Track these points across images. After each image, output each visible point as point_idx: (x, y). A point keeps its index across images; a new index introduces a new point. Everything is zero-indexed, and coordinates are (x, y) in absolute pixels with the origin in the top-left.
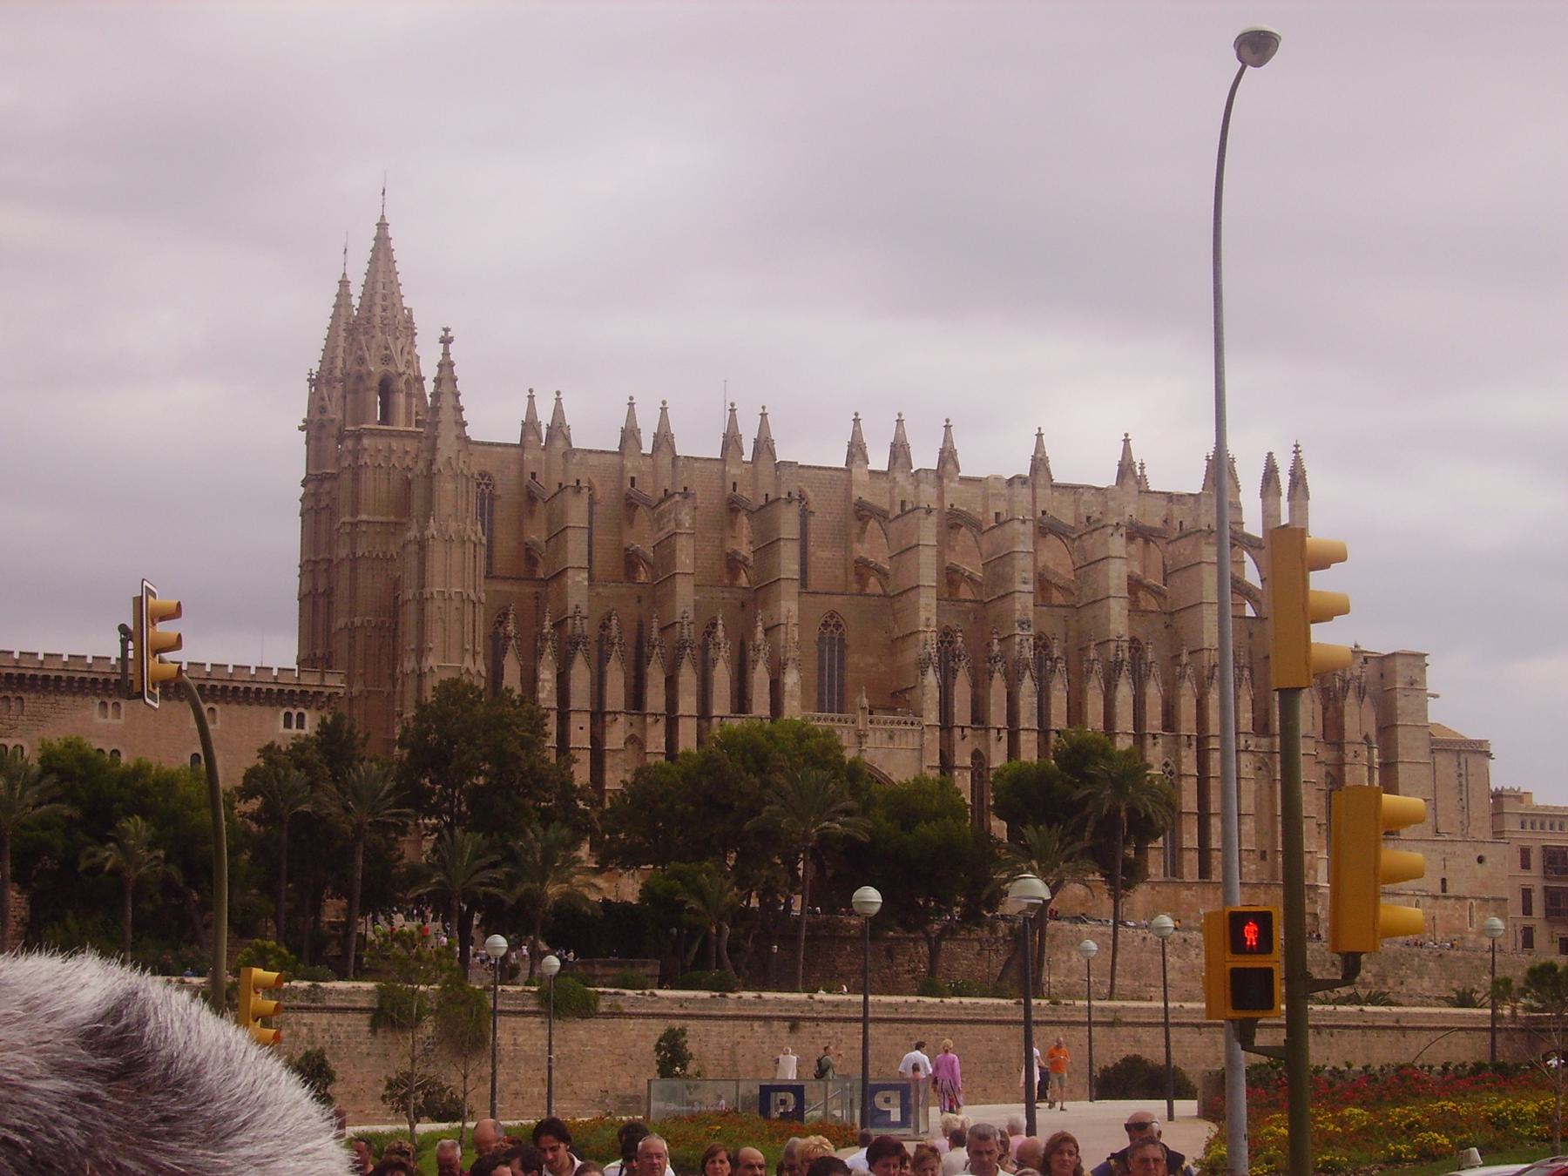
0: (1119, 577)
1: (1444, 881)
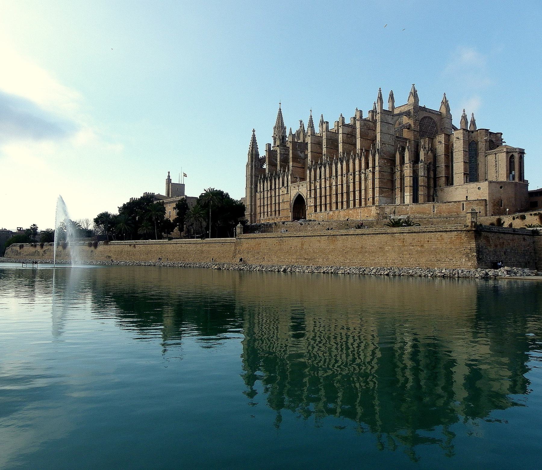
1: (467, 197)
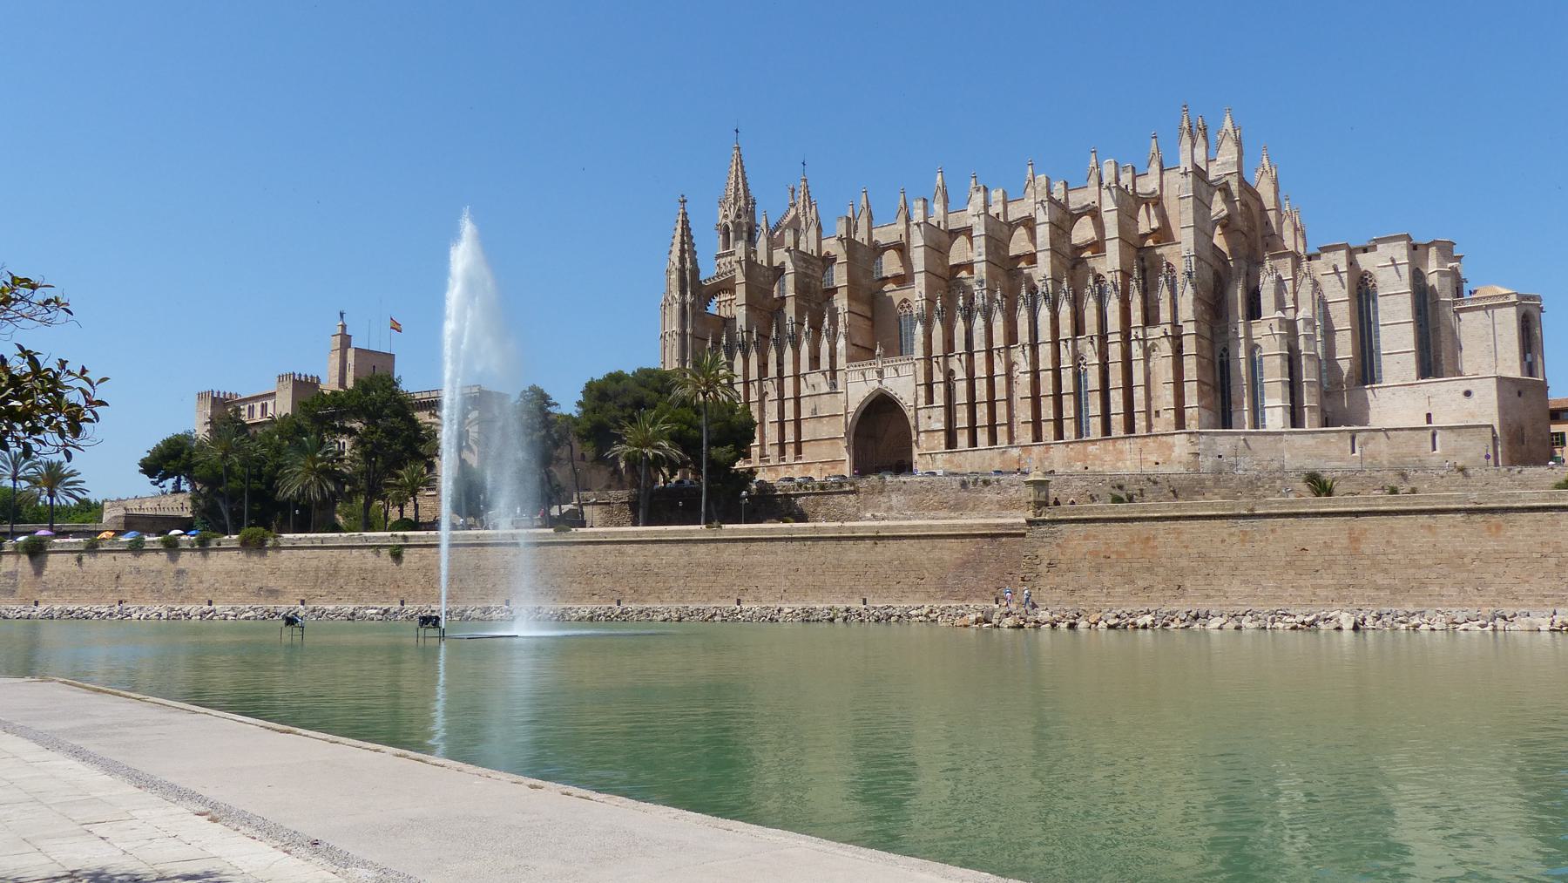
0: (1043, 236)
1: (1429, 416)
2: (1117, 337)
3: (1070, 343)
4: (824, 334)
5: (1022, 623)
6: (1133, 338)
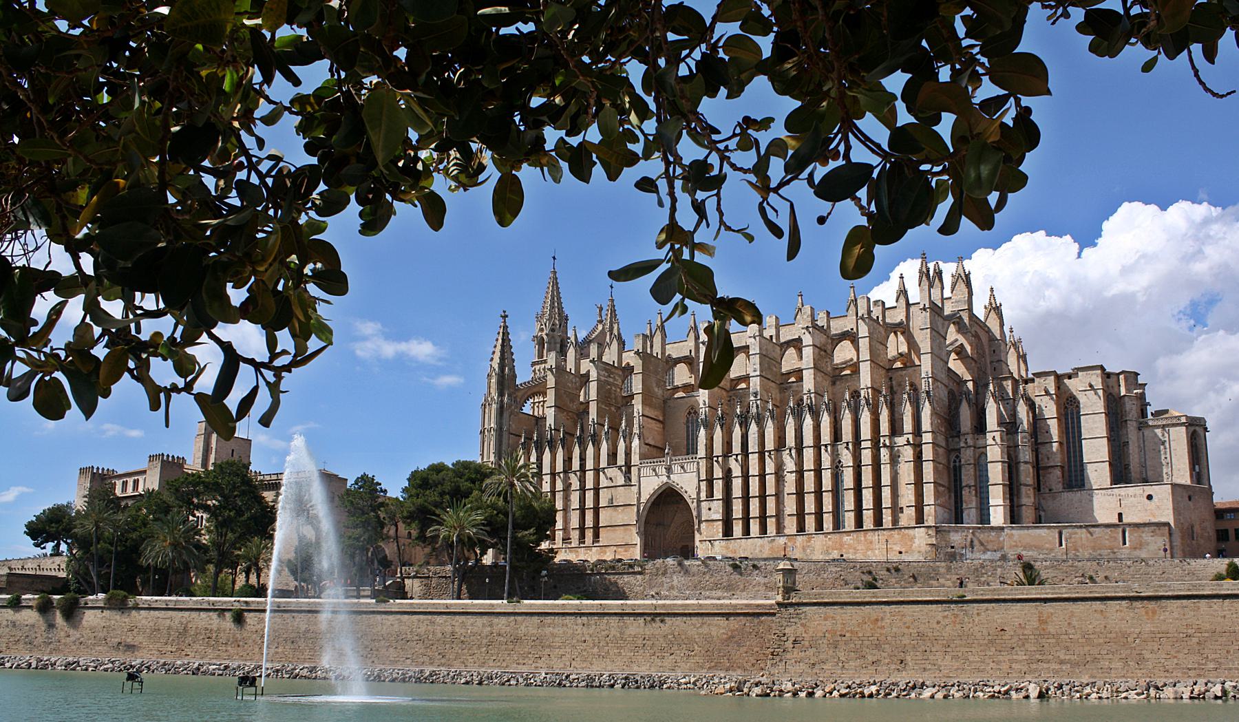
0: (808, 357)
1: (1120, 515)
2: (868, 444)
3: (829, 448)
4: (621, 434)
5: (768, 691)
6: (881, 445)
